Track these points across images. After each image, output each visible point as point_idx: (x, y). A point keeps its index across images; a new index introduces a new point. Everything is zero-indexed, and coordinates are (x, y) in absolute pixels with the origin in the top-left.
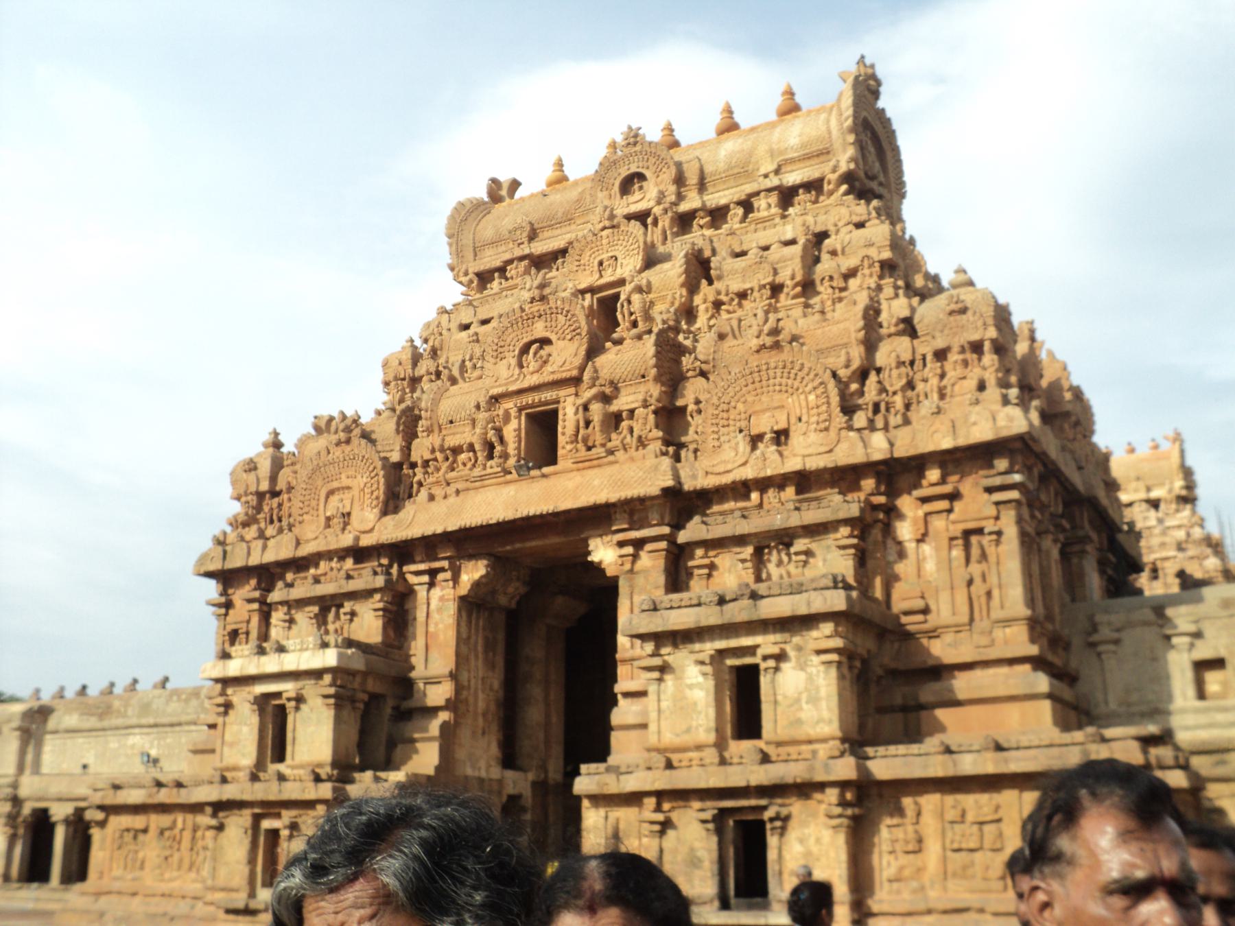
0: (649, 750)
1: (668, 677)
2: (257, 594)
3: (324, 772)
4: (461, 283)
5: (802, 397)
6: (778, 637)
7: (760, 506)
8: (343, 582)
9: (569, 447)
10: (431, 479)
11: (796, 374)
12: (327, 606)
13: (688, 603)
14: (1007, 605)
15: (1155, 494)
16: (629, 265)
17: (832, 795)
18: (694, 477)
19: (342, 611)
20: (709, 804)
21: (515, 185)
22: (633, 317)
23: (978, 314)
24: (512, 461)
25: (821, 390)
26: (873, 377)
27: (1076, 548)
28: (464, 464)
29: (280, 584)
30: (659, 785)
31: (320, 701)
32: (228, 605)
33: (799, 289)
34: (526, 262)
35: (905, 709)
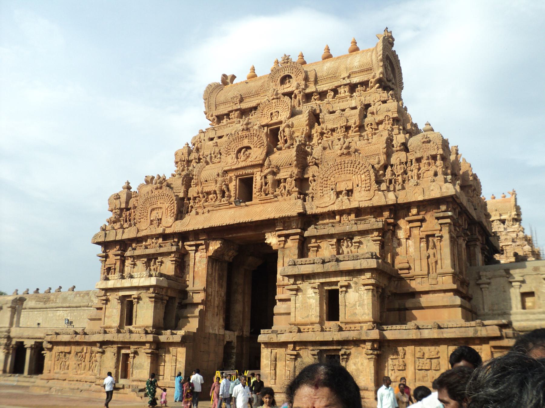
2: (119, 252)
3: (149, 330)
4: (209, 120)
5: (359, 176)
6: (347, 278)
7: (340, 222)
8: (158, 248)
9: (258, 194)
10: (197, 205)
11: (357, 166)
12: (150, 258)
13: (309, 263)
14: (444, 267)
15: (503, 217)
16: (284, 115)
17: (369, 345)
18: (312, 208)
19: (157, 261)
21: (234, 77)
22: (285, 138)
23: (435, 143)
24: (232, 199)
26: (389, 168)
27: (472, 243)
28: (212, 199)
29: (130, 248)
30: (295, 339)
31: (148, 299)
32: (107, 257)
33: (357, 128)
35: (399, 310)
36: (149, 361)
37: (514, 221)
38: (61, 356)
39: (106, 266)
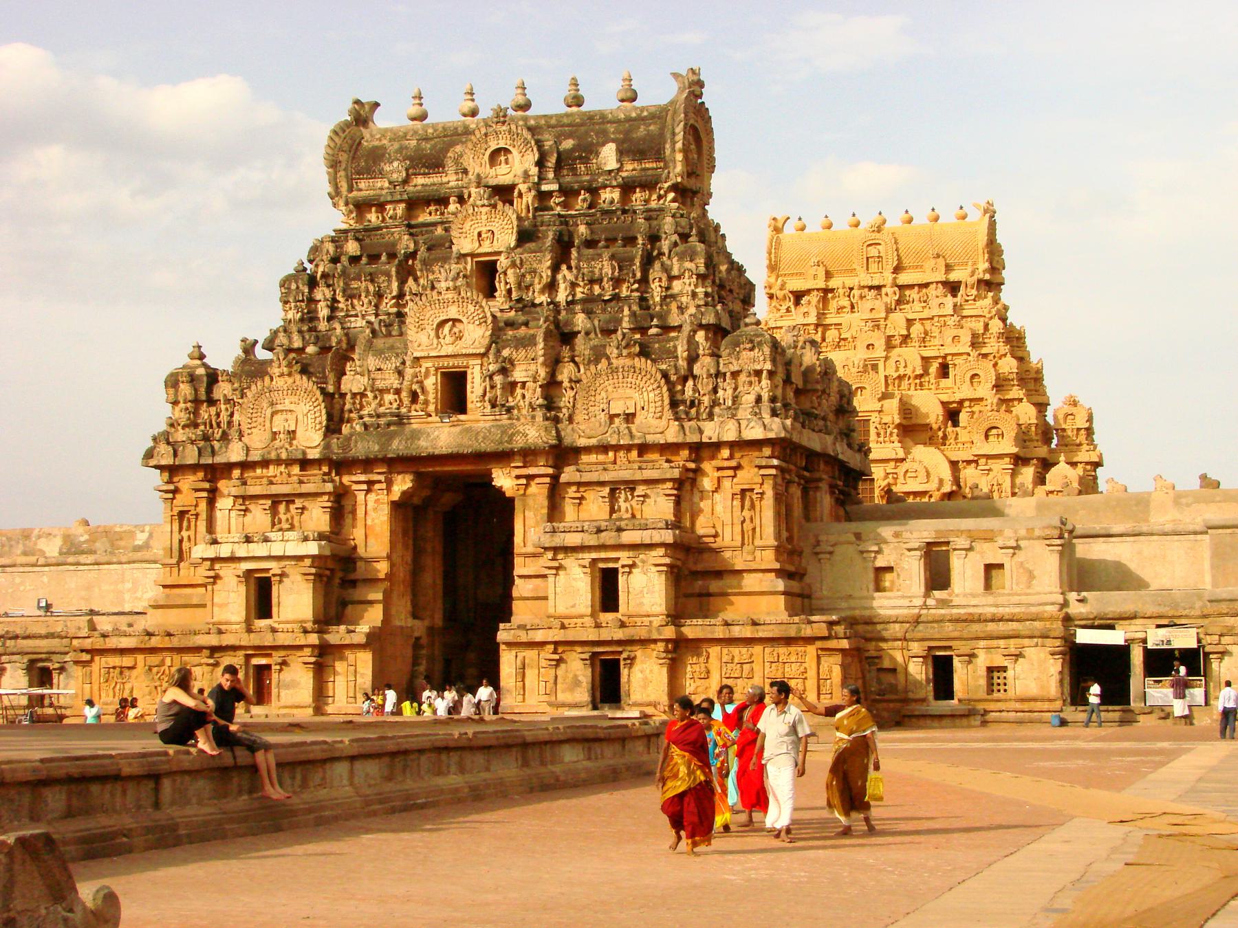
0: (548, 617)
1: (560, 572)
2: (207, 485)
3: (309, 626)
5: (645, 394)
6: (631, 554)
9: (479, 405)
14: (764, 537)
15: (953, 277)
17: (661, 646)
20: (587, 649)
21: (377, 105)
24: (431, 408)
25: (657, 392)
26: (690, 383)
27: (813, 485)
30: (556, 639)
31: (299, 578)
34: (403, 206)
35: (700, 595)
36: (311, 674)
37: (983, 287)
38: (111, 675)
39: (175, 508)
